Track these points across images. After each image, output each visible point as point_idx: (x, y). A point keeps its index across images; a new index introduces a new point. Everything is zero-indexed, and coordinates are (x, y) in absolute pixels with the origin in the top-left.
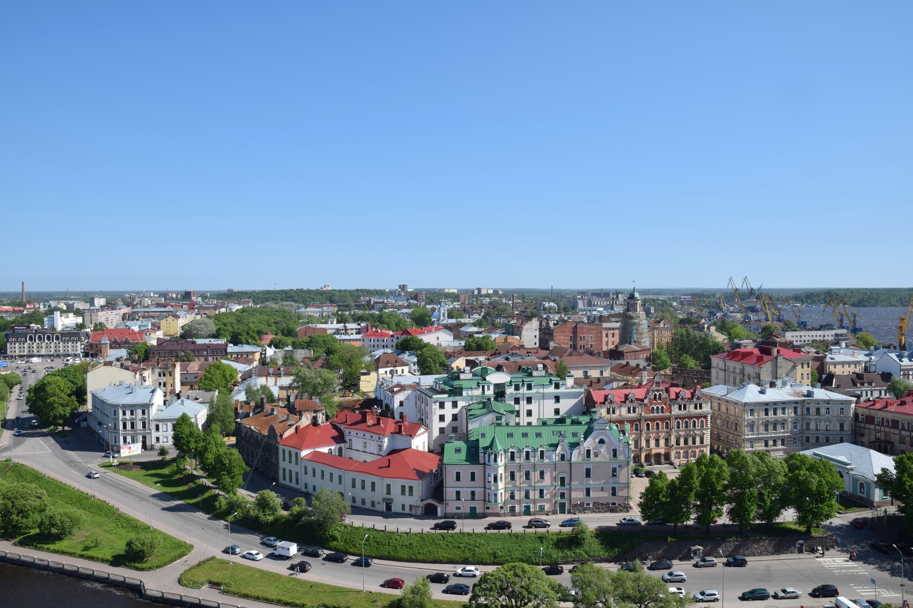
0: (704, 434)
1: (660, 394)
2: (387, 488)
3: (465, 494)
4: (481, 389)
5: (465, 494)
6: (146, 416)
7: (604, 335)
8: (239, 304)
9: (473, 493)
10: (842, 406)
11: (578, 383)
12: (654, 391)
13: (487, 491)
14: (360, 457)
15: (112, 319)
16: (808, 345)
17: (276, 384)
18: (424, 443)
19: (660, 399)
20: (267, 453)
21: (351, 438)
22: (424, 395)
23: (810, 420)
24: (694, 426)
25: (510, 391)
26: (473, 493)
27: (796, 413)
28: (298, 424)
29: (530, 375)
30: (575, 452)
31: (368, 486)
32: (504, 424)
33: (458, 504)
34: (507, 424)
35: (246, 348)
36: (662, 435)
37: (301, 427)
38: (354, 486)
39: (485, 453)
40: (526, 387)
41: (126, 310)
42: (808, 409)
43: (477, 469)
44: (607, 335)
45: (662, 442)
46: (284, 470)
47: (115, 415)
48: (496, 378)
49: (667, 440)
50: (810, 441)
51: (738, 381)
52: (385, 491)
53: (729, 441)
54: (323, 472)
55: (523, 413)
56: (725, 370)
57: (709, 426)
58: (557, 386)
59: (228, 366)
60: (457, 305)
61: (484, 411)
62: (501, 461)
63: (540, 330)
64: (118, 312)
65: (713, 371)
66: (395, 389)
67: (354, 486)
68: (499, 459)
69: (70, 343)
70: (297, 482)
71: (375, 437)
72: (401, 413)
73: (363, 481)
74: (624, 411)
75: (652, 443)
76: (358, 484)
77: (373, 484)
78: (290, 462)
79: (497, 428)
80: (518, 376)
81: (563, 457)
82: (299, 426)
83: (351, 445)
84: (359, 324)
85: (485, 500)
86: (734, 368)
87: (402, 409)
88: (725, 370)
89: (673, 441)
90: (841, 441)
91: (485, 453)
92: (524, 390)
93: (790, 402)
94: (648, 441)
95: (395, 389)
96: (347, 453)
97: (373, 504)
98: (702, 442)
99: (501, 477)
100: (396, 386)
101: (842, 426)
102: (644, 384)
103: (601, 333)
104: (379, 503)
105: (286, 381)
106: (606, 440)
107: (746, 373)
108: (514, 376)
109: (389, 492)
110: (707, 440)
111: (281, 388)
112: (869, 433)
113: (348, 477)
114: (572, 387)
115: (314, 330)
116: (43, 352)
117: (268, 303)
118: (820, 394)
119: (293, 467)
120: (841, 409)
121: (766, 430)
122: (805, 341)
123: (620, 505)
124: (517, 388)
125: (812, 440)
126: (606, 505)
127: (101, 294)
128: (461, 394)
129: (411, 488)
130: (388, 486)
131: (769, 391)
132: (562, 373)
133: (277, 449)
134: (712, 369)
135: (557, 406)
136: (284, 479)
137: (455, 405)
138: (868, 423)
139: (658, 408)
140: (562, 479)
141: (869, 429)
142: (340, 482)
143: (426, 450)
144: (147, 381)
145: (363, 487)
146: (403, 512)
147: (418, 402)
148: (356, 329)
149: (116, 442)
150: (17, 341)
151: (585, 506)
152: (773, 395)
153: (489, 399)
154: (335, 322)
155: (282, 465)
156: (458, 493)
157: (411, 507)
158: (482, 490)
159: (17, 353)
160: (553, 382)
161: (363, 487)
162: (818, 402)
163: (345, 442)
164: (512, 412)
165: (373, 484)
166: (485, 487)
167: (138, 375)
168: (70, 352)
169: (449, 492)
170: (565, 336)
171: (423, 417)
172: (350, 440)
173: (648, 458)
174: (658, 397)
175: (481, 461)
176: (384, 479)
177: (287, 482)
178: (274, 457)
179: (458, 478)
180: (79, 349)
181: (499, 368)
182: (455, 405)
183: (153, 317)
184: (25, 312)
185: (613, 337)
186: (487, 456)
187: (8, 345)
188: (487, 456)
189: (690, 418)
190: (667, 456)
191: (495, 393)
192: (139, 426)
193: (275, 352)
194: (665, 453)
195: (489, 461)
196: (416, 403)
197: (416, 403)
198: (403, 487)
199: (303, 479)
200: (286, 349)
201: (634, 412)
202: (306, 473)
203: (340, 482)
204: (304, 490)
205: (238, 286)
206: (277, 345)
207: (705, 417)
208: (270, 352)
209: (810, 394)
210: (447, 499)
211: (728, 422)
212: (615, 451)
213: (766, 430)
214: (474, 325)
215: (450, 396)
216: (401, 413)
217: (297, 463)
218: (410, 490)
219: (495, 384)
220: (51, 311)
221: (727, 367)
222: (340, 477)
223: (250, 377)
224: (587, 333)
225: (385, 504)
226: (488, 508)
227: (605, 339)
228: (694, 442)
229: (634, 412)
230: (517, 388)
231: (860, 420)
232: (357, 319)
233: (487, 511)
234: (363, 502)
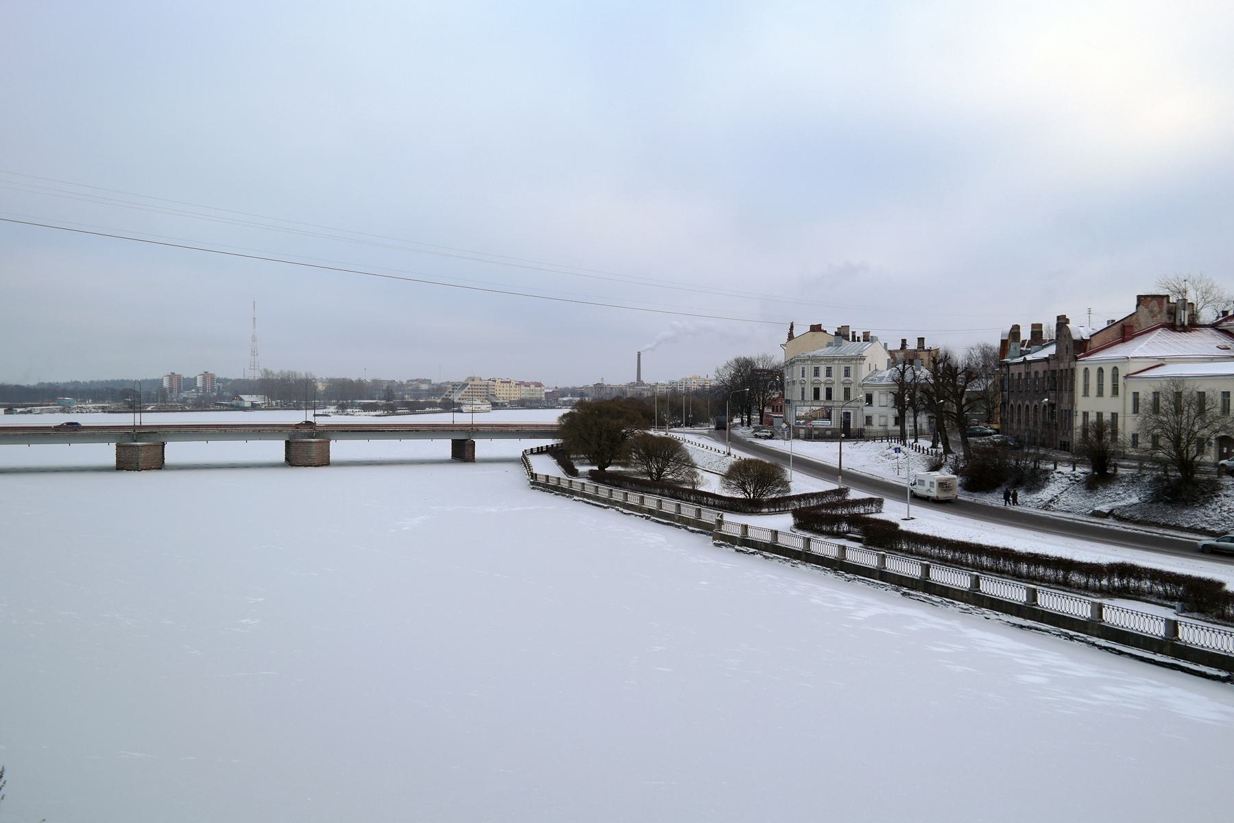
6: (851, 379)
47: (803, 376)
78: (1100, 393)
192: (838, 394)
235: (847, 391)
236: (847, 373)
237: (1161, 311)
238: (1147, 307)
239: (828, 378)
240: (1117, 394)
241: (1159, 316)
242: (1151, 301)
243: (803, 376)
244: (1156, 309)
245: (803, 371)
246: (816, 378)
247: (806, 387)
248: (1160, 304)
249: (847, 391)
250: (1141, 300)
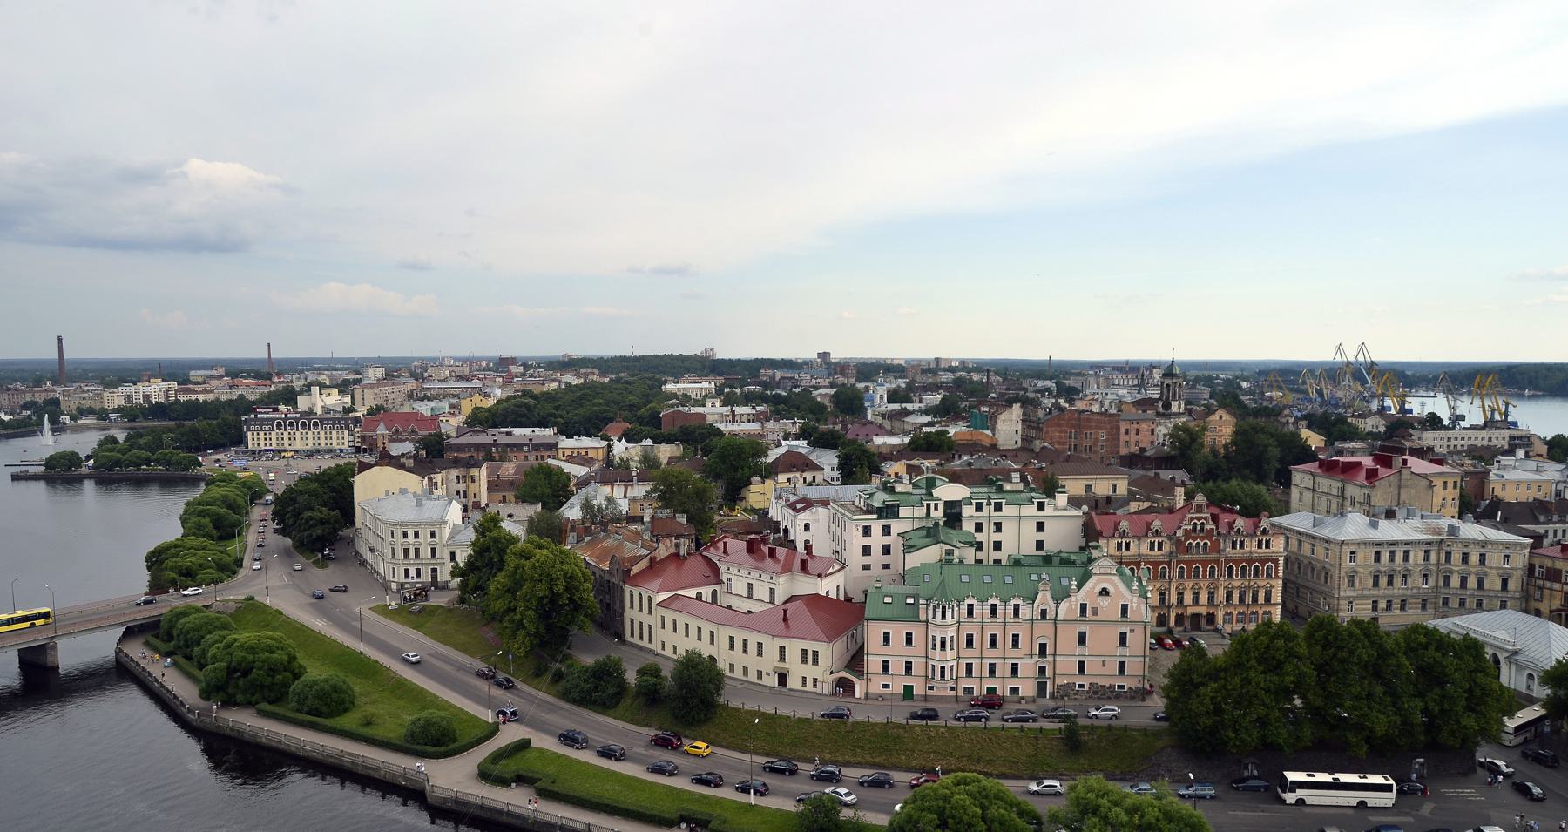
0: (1272, 587)
1: (1202, 524)
3: (897, 666)
4: (925, 508)
5: (897, 666)
6: (437, 540)
7: (1123, 430)
8: (578, 377)
9: (909, 666)
10: (1507, 552)
11: (1074, 502)
12: (1192, 519)
13: (931, 662)
14: (745, 606)
15: (394, 396)
16: (1459, 453)
17: (625, 496)
18: (838, 587)
19: (1202, 529)
20: (607, 597)
21: (730, 576)
22: (840, 516)
23: (1451, 572)
24: (1256, 574)
25: (968, 511)
26: (909, 666)
27: (1427, 558)
28: (653, 554)
29: (1000, 489)
30: (1064, 606)
31: (752, 648)
32: (957, 561)
33: (886, 680)
34: (961, 562)
35: (586, 442)
36: (1204, 584)
38: (732, 648)
39: (928, 605)
40: (992, 507)
41: (411, 385)
42: (1448, 555)
43: (916, 630)
44: (1127, 432)
45: (1203, 598)
46: (632, 620)
47: (393, 537)
48: (949, 491)
49: (1211, 595)
50: (1450, 606)
51: (1334, 507)
52: (777, 657)
53: (1314, 600)
54: (687, 625)
55: (988, 546)
56: (1314, 490)
57: (1281, 574)
58: (1041, 507)
59: (559, 468)
60: (902, 383)
61: (927, 541)
62: (953, 618)
63: (1024, 421)
64: (402, 388)
65: (1294, 490)
66: (799, 506)
67: (732, 648)
68: (949, 615)
69: (334, 432)
70: (651, 641)
71: (766, 577)
72: (807, 542)
73: (745, 642)
74: (1145, 549)
75: (1188, 598)
76: (738, 645)
77: (760, 645)
78: (641, 610)
79: (945, 568)
80: (981, 490)
81: (1044, 613)
82: (655, 558)
83: (730, 586)
84: (754, 408)
85: (927, 677)
86: (1329, 487)
87: (807, 536)
88: (1314, 490)
89: (1221, 595)
90: (1503, 606)
91: (928, 605)
92: (988, 511)
93: (1417, 543)
94: (1181, 595)
95: (799, 506)
96: (723, 600)
97: (760, 674)
98: (1268, 599)
99: (952, 641)
100: (802, 500)
101: (1505, 583)
102: (1178, 506)
103: (1118, 428)
104: (768, 674)
105: (639, 491)
106: (1112, 590)
107: (1348, 495)
108: (976, 490)
109: (782, 658)
110: (1277, 596)
111: (633, 500)
112: (1551, 595)
113: (723, 634)
114: (1065, 510)
115: (687, 415)
116: (298, 445)
117: (622, 375)
118: (1471, 530)
119: (647, 620)
120: (1505, 556)
121: (1376, 584)
122: (1455, 446)
123: (1130, 688)
124: (979, 507)
125: (1454, 603)
126: (1110, 687)
127: (378, 362)
128: (896, 516)
129: (816, 653)
130: (782, 650)
131: (1384, 524)
132: (1050, 489)
133: (622, 590)
134: (1292, 487)
135: (1040, 536)
136: (632, 635)
137: (887, 531)
138: (1549, 580)
139: (1198, 543)
140: (1043, 647)
141: (1551, 589)
142: (712, 642)
143: (842, 598)
144: (439, 489)
145: (745, 651)
146: (804, 688)
147: (833, 526)
148: (749, 415)
149: (394, 576)
150: (261, 430)
151: (1077, 688)
152: (1388, 530)
153: (937, 524)
154: (718, 404)
155: (630, 613)
156: (886, 666)
157: (815, 680)
158: (924, 660)
159: (263, 447)
160: (1035, 501)
161: (745, 651)
162: (1466, 543)
163: (720, 582)
164: (970, 544)
165: (760, 645)
166: (927, 657)
167: (426, 481)
168: (335, 446)
169: (873, 663)
170: (1061, 432)
171: (839, 549)
172: (729, 580)
173: (1180, 619)
174: (1198, 528)
175: (923, 617)
177: (636, 640)
178: (618, 603)
179: (887, 637)
180: (346, 441)
181: (955, 478)
182: (887, 531)
183: (454, 396)
184: (273, 389)
185: (1137, 434)
186: (931, 608)
187: (250, 434)
188: (931, 608)
189: (1250, 562)
190: (1211, 618)
191: (946, 514)
192: (426, 553)
193: (627, 448)
194: (1208, 614)
195: (934, 618)
196: (829, 527)
197: (829, 527)
198: (804, 652)
199: (659, 635)
200: (643, 443)
201: (1160, 549)
203: (712, 642)
204: (660, 651)
205: (578, 352)
206: (631, 437)
207: (1276, 562)
208: (620, 448)
209: (1453, 530)
211: (1313, 569)
212: (1124, 608)
213: (1376, 584)
214: (926, 412)
215: (879, 518)
216: (807, 542)
217: (650, 612)
219: (947, 503)
220: (307, 389)
221: (1316, 486)
222: (712, 633)
223: (588, 484)
224: (1096, 427)
225: (777, 675)
226: (931, 688)
227: (1124, 437)
228: (1255, 599)
229: (1160, 549)
230: (979, 507)
231: (1537, 574)
232: (747, 399)
233: (930, 693)
234: (745, 670)
235: (433, 551)
236: (433, 535)
239: (417, 540)
243: (393, 537)
244: (669, 545)
245: (392, 533)
246: (405, 540)
247: (395, 547)
248: (671, 541)
249: (433, 551)
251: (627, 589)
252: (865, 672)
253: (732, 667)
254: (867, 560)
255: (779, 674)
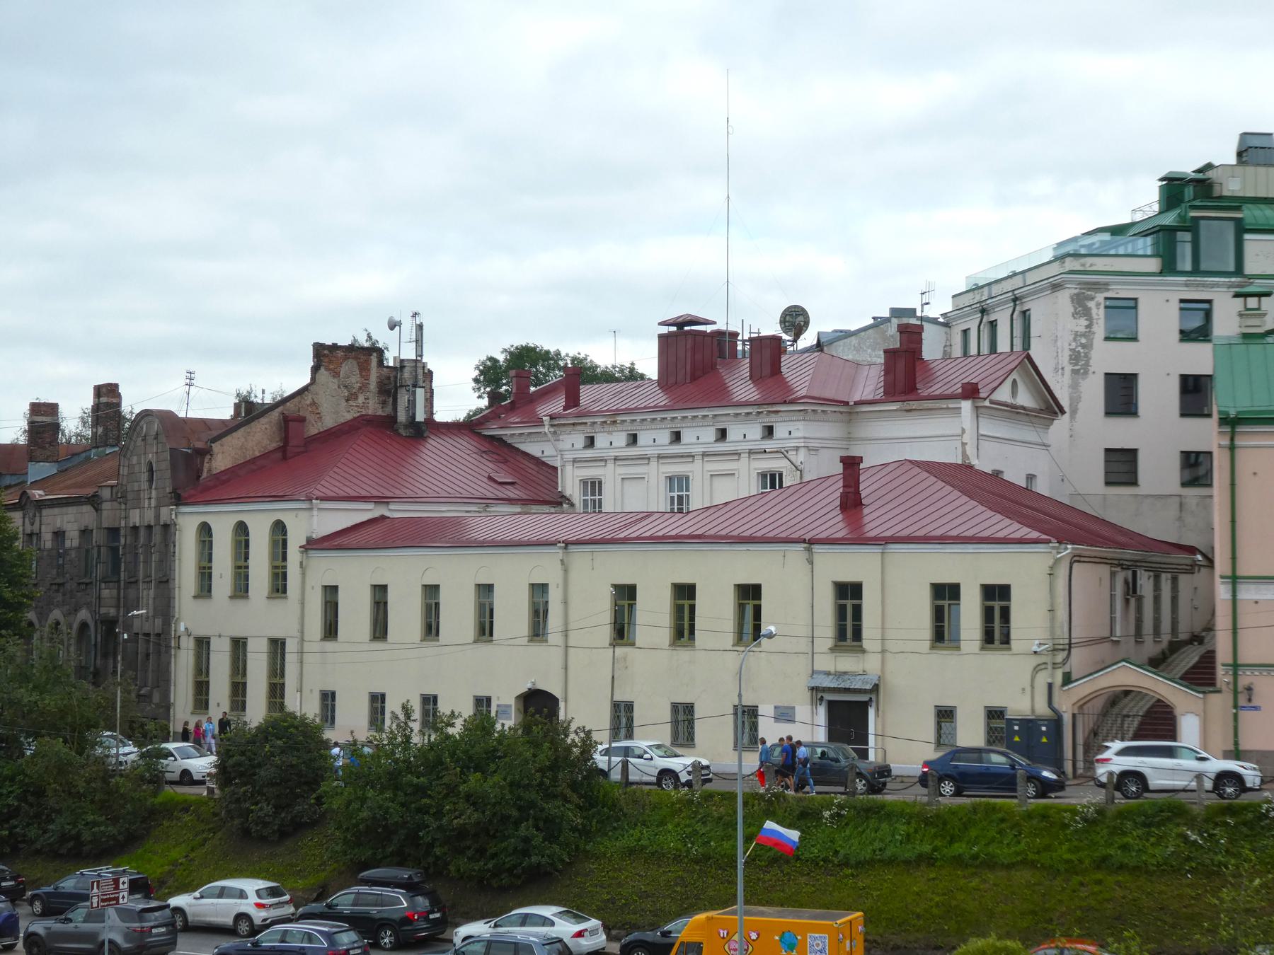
2: (841, 612)
37: (313, 430)
71: (745, 433)
77: (749, 594)
129: (996, 595)
130: (849, 593)
165: (749, 594)
176: (816, 548)
198: (946, 594)
202: (331, 631)
203: (538, 630)
210: (1246, 656)
218: (988, 614)
237: (363, 388)
238: (336, 375)
240: (285, 591)
241: (361, 399)
242: (345, 359)
244: (355, 380)
248: (364, 368)
250: (324, 355)
251: (188, 522)
252: (1223, 654)
253: (623, 717)
254: (1122, 433)
255: (832, 706)
